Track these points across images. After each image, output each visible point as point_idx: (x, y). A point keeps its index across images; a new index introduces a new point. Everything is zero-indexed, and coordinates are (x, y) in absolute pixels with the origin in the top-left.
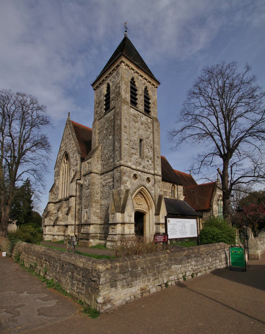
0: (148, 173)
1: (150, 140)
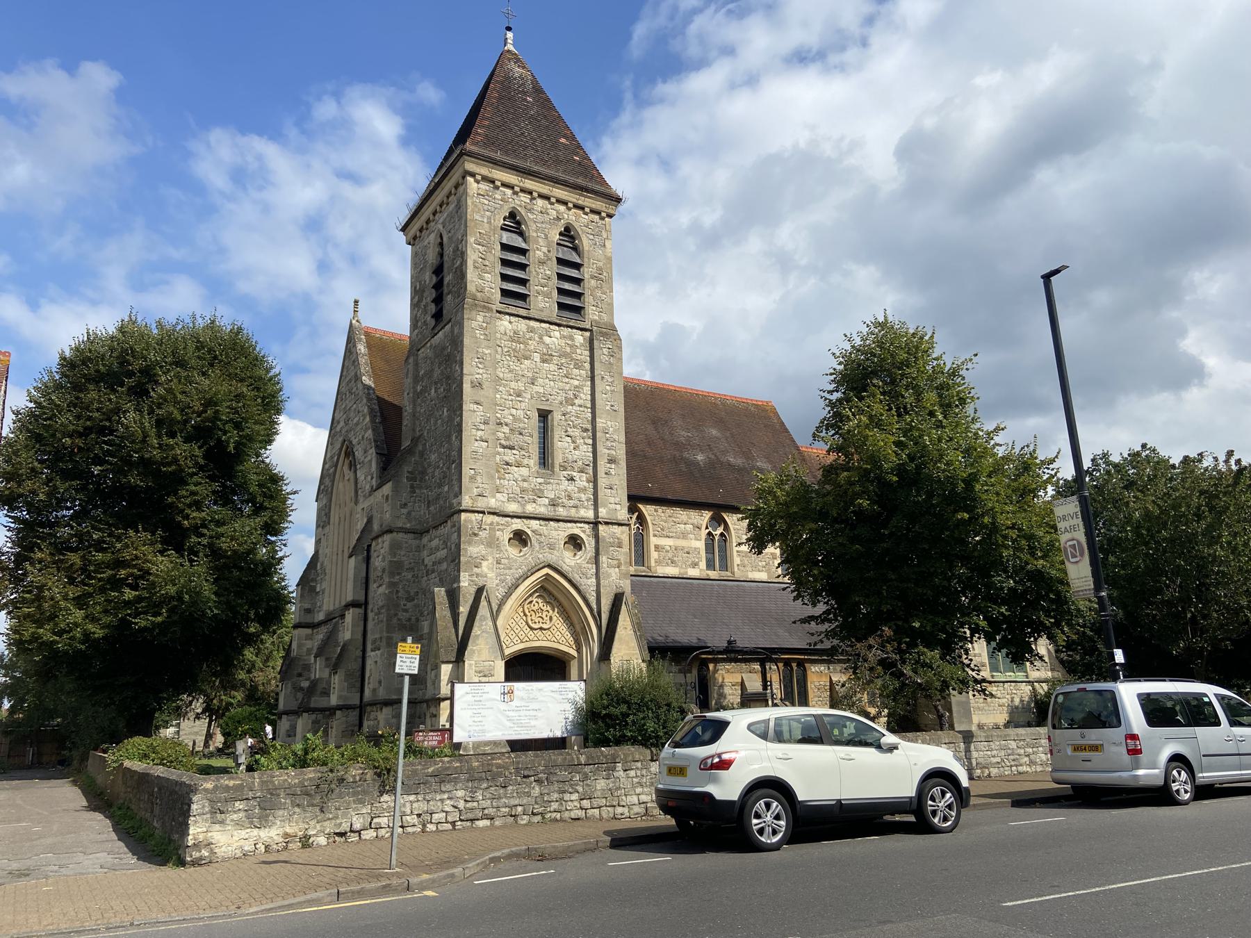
1: (580, 406)
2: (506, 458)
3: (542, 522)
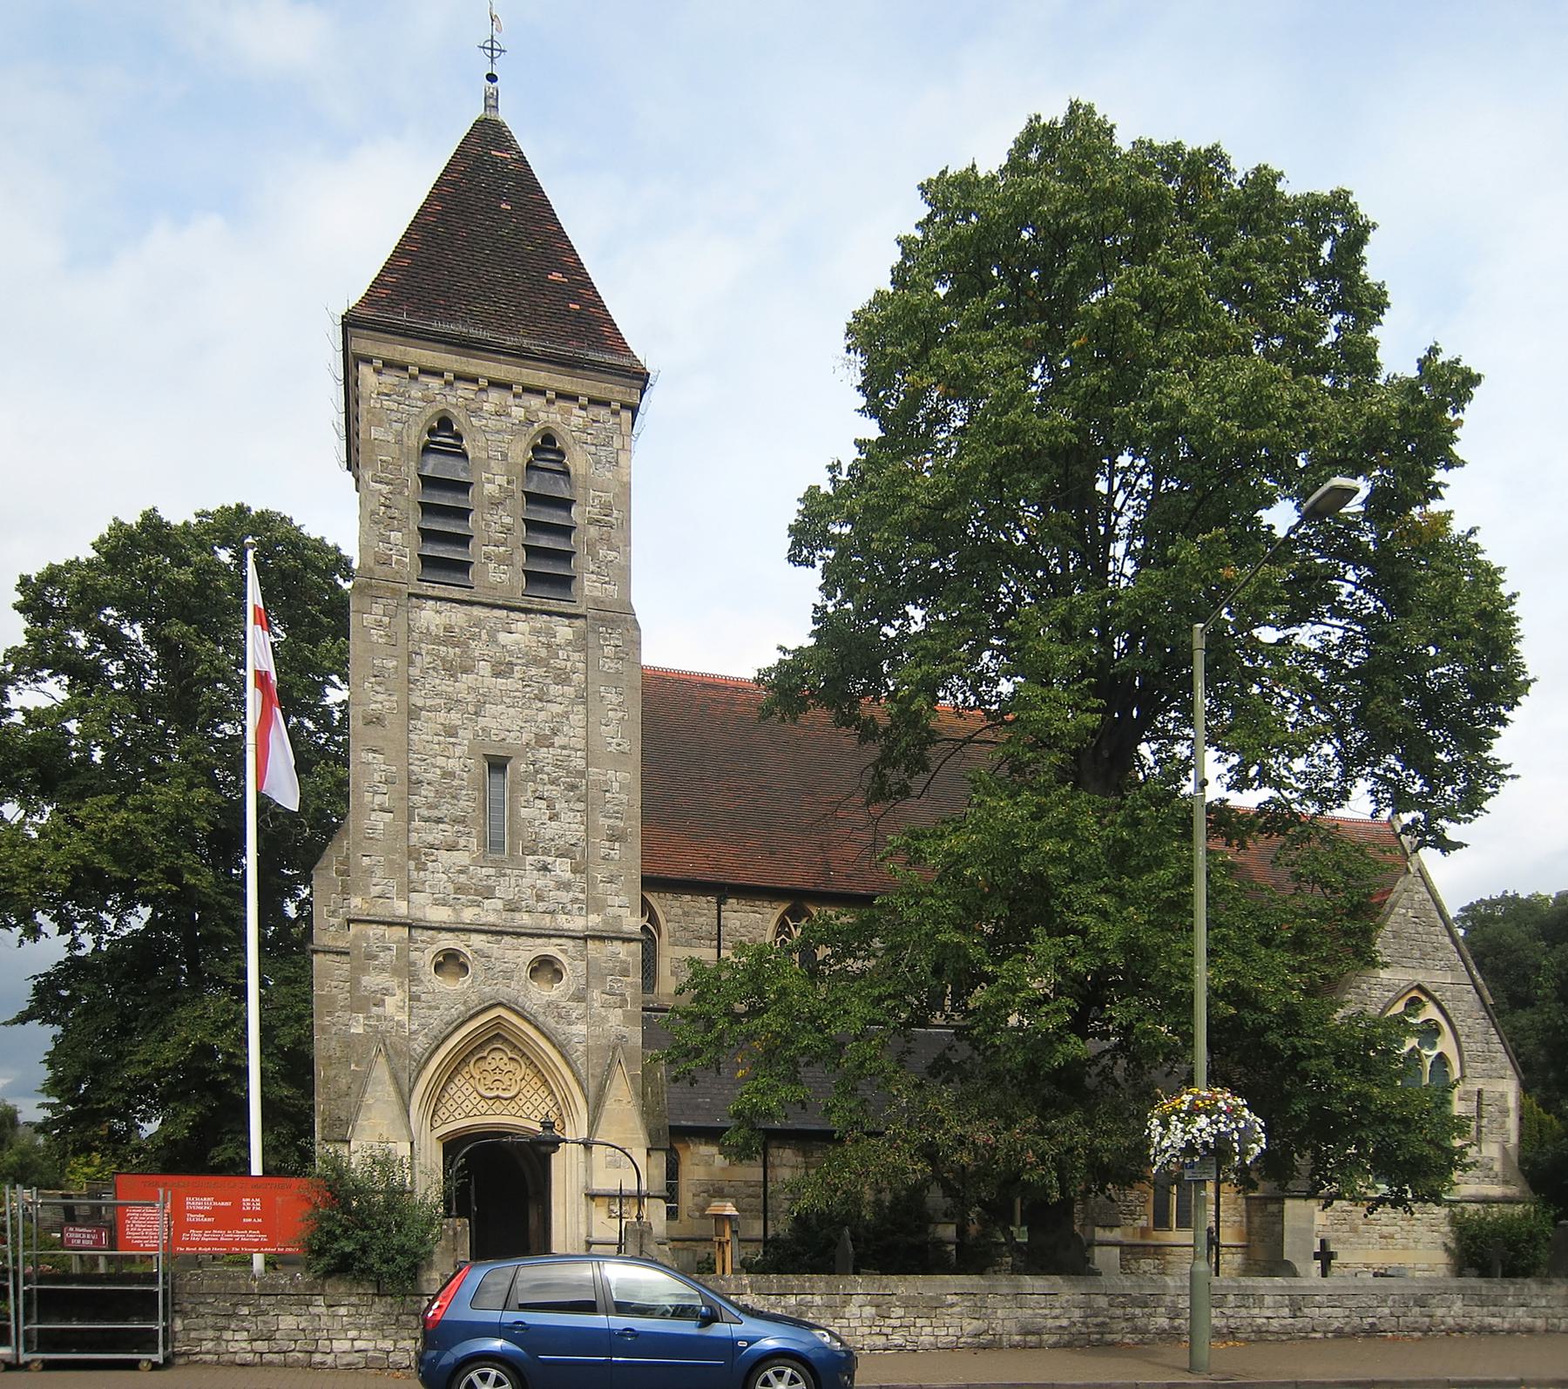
0: (540, 936)
1: (563, 747)
2: (430, 839)
3: (490, 937)
